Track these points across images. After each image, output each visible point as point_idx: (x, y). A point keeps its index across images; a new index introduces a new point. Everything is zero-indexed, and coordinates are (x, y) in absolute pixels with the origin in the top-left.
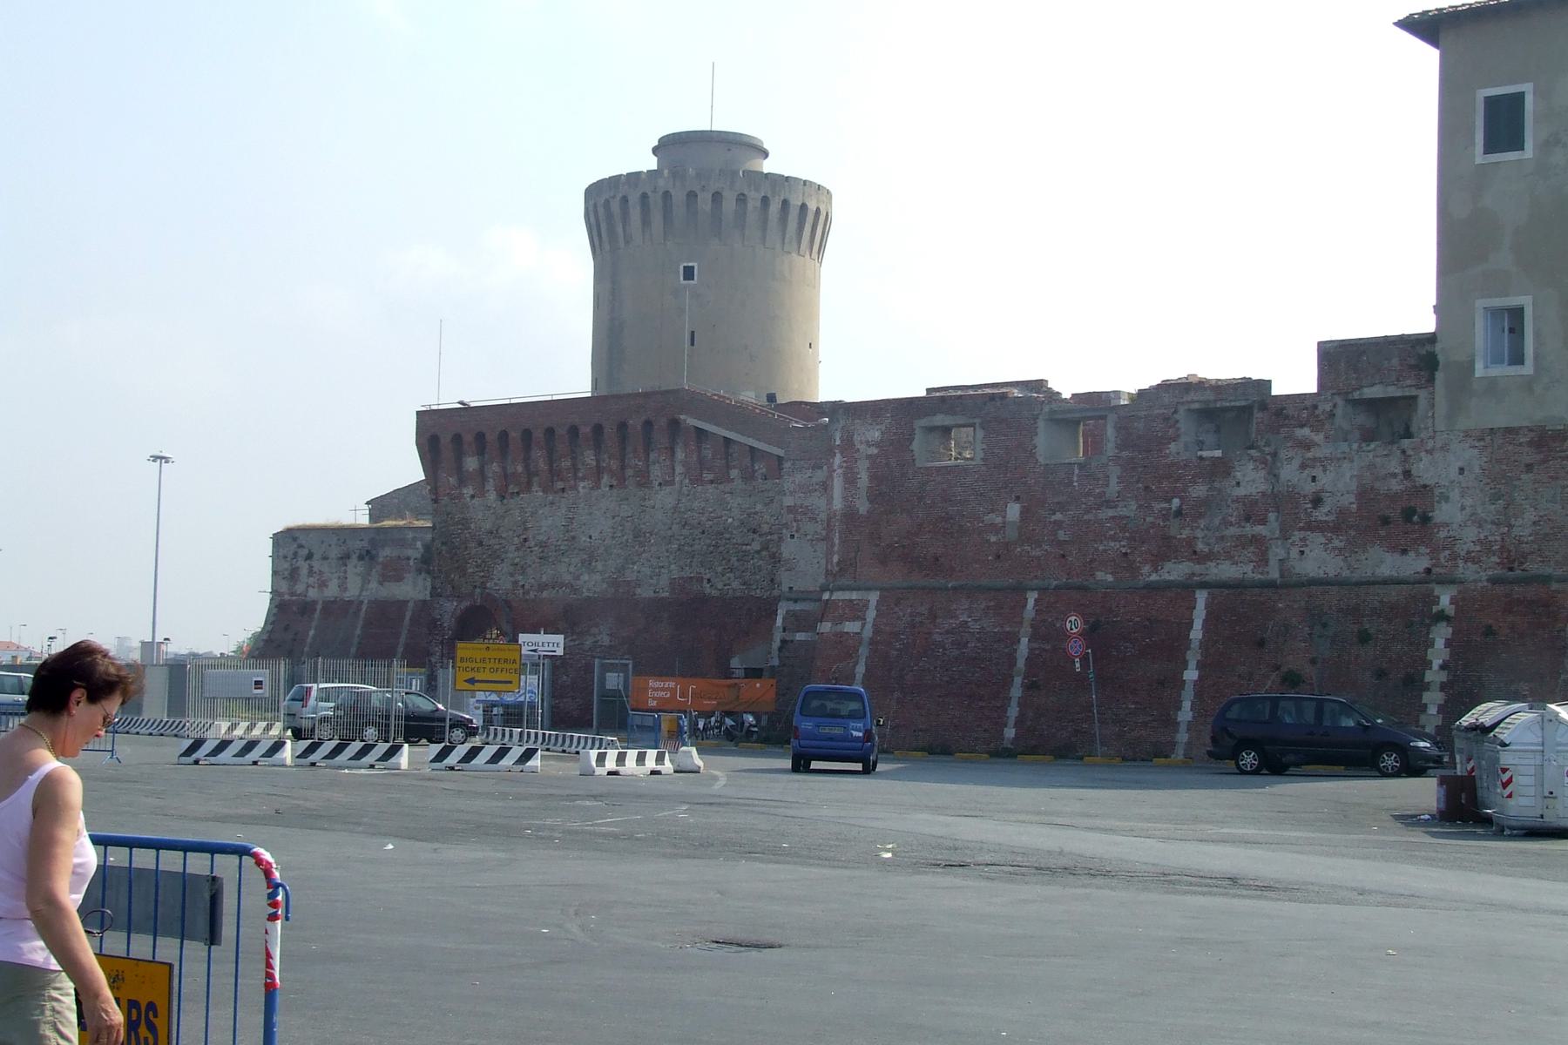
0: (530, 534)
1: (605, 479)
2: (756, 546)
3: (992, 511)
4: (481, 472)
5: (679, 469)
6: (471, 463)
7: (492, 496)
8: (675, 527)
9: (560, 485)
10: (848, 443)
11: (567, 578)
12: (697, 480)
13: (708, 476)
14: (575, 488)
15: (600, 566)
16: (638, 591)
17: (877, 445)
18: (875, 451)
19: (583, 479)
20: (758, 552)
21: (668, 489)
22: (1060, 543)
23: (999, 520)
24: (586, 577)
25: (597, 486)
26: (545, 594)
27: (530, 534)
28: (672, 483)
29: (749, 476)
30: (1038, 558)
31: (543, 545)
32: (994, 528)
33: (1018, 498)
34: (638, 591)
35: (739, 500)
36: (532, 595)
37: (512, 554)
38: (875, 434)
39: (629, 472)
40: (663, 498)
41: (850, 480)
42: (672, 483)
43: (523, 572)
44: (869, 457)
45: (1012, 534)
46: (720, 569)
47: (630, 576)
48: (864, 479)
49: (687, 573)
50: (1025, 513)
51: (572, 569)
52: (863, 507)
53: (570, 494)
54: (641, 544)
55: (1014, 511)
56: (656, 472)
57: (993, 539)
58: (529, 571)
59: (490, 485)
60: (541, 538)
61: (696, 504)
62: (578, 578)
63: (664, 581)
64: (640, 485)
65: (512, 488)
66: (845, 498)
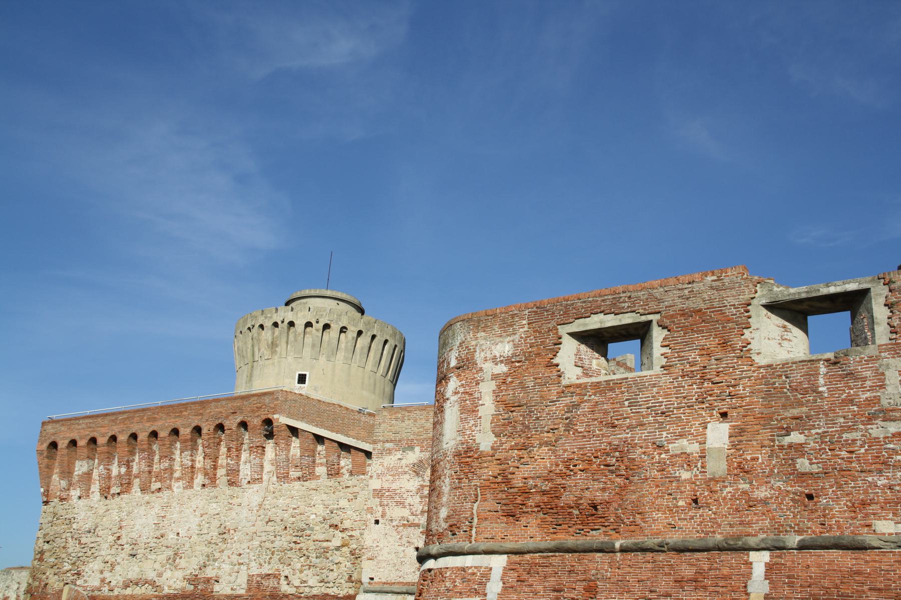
1: (199, 479)
2: (337, 542)
3: (681, 436)
4: (88, 474)
5: (268, 467)
6: (80, 467)
7: (96, 496)
8: (259, 523)
9: (156, 486)
10: (466, 364)
11: (151, 575)
12: (284, 477)
13: (294, 474)
14: (169, 488)
16: (217, 588)
17: (508, 361)
18: (503, 368)
19: (178, 479)
20: (338, 549)
21: (256, 487)
22: (802, 476)
23: (693, 448)
24: (168, 574)
25: (190, 485)
26: (128, 591)
27: (123, 532)
28: (260, 480)
29: (334, 472)
30: (765, 502)
32: (687, 461)
33: (724, 415)
34: (217, 588)
35: (324, 497)
36: (116, 593)
37: (105, 551)
38: (505, 348)
39: (221, 472)
40: (252, 495)
41: (470, 409)
42: (260, 480)
44: (495, 377)
45: (717, 466)
46: (298, 566)
47: (210, 573)
48: (488, 407)
49: (266, 570)
50: (737, 434)
51: (157, 566)
52: (486, 441)
53: (166, 493)
55: (718, 434)
56: (245, 471)
57: (685, 475)
58: (117, 568)
59: (95, 488)
61: (281, 501)
62: (160, 575)
63: (242, 580)
64: (231, 483)
65: (115, 490)
66: (461, 432)
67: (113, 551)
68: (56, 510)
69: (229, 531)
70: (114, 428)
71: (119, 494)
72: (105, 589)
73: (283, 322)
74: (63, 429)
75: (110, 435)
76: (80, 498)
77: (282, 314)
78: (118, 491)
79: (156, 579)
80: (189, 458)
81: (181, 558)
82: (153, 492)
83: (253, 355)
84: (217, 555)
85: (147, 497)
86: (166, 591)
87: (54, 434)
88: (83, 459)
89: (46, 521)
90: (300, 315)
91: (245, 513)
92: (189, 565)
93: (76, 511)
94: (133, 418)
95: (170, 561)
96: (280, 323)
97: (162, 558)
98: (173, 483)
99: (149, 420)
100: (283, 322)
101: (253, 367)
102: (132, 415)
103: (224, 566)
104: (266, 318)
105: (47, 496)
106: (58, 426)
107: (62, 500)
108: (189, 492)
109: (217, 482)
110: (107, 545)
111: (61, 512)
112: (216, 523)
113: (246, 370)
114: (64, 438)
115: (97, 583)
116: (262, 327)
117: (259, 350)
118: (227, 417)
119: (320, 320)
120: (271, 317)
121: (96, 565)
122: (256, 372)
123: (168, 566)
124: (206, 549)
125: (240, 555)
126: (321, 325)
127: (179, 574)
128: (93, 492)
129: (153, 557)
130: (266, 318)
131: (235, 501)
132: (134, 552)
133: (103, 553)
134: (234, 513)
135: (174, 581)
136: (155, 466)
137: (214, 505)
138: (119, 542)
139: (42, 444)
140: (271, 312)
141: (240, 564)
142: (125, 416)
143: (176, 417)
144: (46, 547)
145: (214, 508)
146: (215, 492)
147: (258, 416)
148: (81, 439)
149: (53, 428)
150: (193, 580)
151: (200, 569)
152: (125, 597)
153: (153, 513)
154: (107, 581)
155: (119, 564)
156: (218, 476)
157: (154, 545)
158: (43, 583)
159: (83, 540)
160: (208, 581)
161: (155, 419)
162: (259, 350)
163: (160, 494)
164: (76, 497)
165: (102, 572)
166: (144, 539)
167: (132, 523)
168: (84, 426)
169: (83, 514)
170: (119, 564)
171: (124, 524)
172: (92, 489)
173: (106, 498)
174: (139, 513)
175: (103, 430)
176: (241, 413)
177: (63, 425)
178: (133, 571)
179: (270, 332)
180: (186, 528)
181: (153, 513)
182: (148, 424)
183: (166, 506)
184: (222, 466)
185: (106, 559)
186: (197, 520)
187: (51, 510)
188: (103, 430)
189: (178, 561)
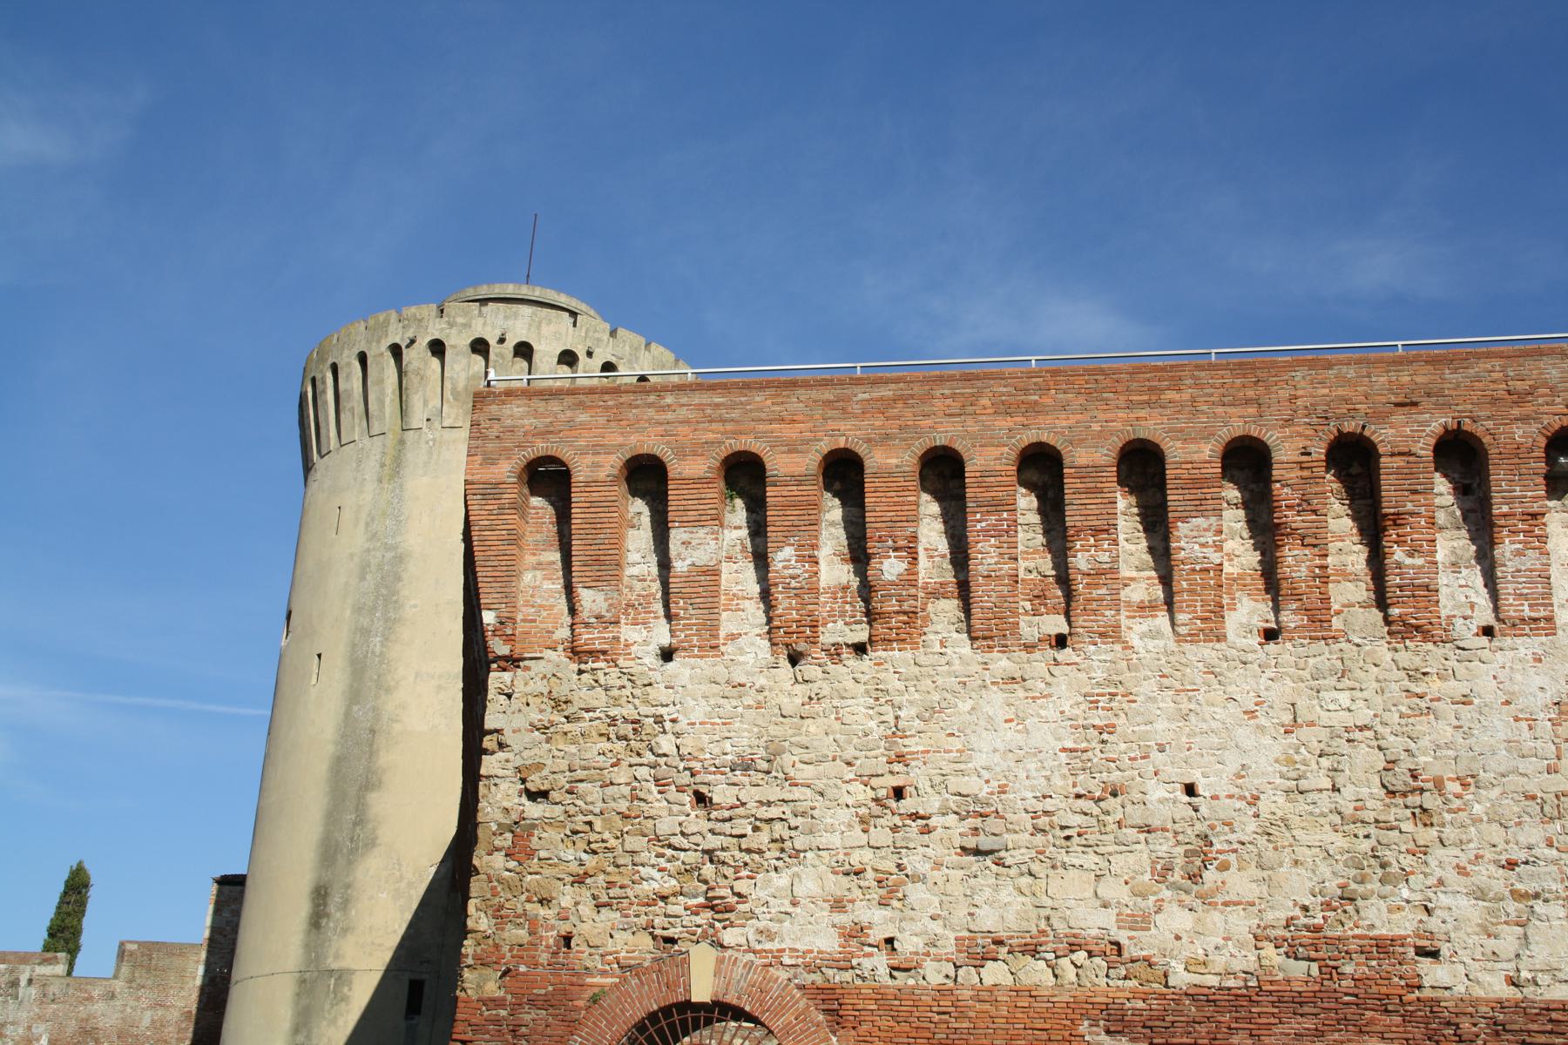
0: (917, 776)
11: (1095, 922)
14: (1111, 634)
15: (1240, 883)
16: (1434, 974)
21: (1527, 646)
24: (1176, 919)
26: (994, 973)
31: (978, 811)
34: (1434, 974)
36: (934, 973)
37: (837, 829)
43: (889, 891)
47: (1383, 917)
51: (1113, 890)
53: (1096, 659)
54: (1423, 815)
56: (1460, 592)
58: (916, 893)
60: (971, 785)
62: (1140, 922)
67: (880, 835)
68: (561, 691)
69: (1439, 784)
70: (842, 426)
71: (860, 649)
72: (879, 963)
73: (502, 341)
74: (583, 417)
75: (825, 446)
76: (667, 655)
77: (500, 322)
78: (862, 635)
79: (1122, 937)
80: (1210, 538)
81: (1224, 867)
82: (1029, 648)
83: (403, 411)
84: (1399, 860)
85: (1002, 664)
86: (1181, 978)
87: (544, 434)
88: (698, 523)
89: (520, 721)
90: (545, 329)
91: (1499, 727)
92: (1297, 889)
93: (659, 693)
94: (927, 398)
95: (1177, 876)
96: (493, 342)
97: (1136, 861)
98: (1124, 622)
99: (1004, 409)
100: (502, 341)
101: (402, 442)
102: (917, 389)
103: (1444, 900)
104: (451, 325)
105: (510, 639)
106: (555, 406)
107: (575, 653)
108: (1207, 651)
109: (1337, 623)
110: (845, 815)
111: (584, 695)
112: (1366, 758)
113: (374, 452)
114: (597, 449)
115: (827, 942)
116: (437, 348)
117: (426, 403)
118: (1381, 417)
119: (597, 351)
120: (467, 326)
121: (813, 880)
122: (415, 456)
123: (1167, 894)
124: (1340, 842)
125: (1511, 865)
126: (598, 362)
127: (1241, 924)
128: (733, 637)
129: (1090, 860)
130: (451, 325)
131: (1434, 686)
132: (985, 842)
133: (835, 840)
134: (1445, 731)
135: (1207, 944)
136: (1022, 564)
137: (1344, 698)
138: (907, 805)
139: (489, 461)
140: (466, 314)
141: (1518, 896)
142: (887, 392)
143: (1130, 405)
144: (534, 810)
145: (1339, 707)
146: (1323, 656)
147: (1524, 419)
148: (681, 454)
149: (536, 414)
150: (1304, 941)
151: (1327, 906)
152: (987, 994)
153: (1051, 713)
154: (877, 935)
155: (916, 878)
156: (1335, 607)
157: (1079, 819)
158: (550, 937)
159: (721, 794)
160: (1383, 947)
161: (1034, 409)
162: (426, 403)
163: (1065, 655)
164: (653, 648)
165: (838, 905)
166: (1023, 795)
167: (956, 744)
168: (683, 413)
169: (699, 711)
170: (916, 878)
171: (913, 745)
172: (728, 623)
173: (794, 659)
174: (991, 717)
175: (789, 432)
176: (1441, 407)
177: (581, 405)
178: (1002, 907)
179: (464, 361)
180: (1233, 766)
181: (1051, 713)
182: (1004, 423)
183: (1115, 692)
184: (1344, 575)
185: (856, 859)
186: (1277, 746)
187: (541, 687)
188: (789, 432)
189: (1210, 875)
